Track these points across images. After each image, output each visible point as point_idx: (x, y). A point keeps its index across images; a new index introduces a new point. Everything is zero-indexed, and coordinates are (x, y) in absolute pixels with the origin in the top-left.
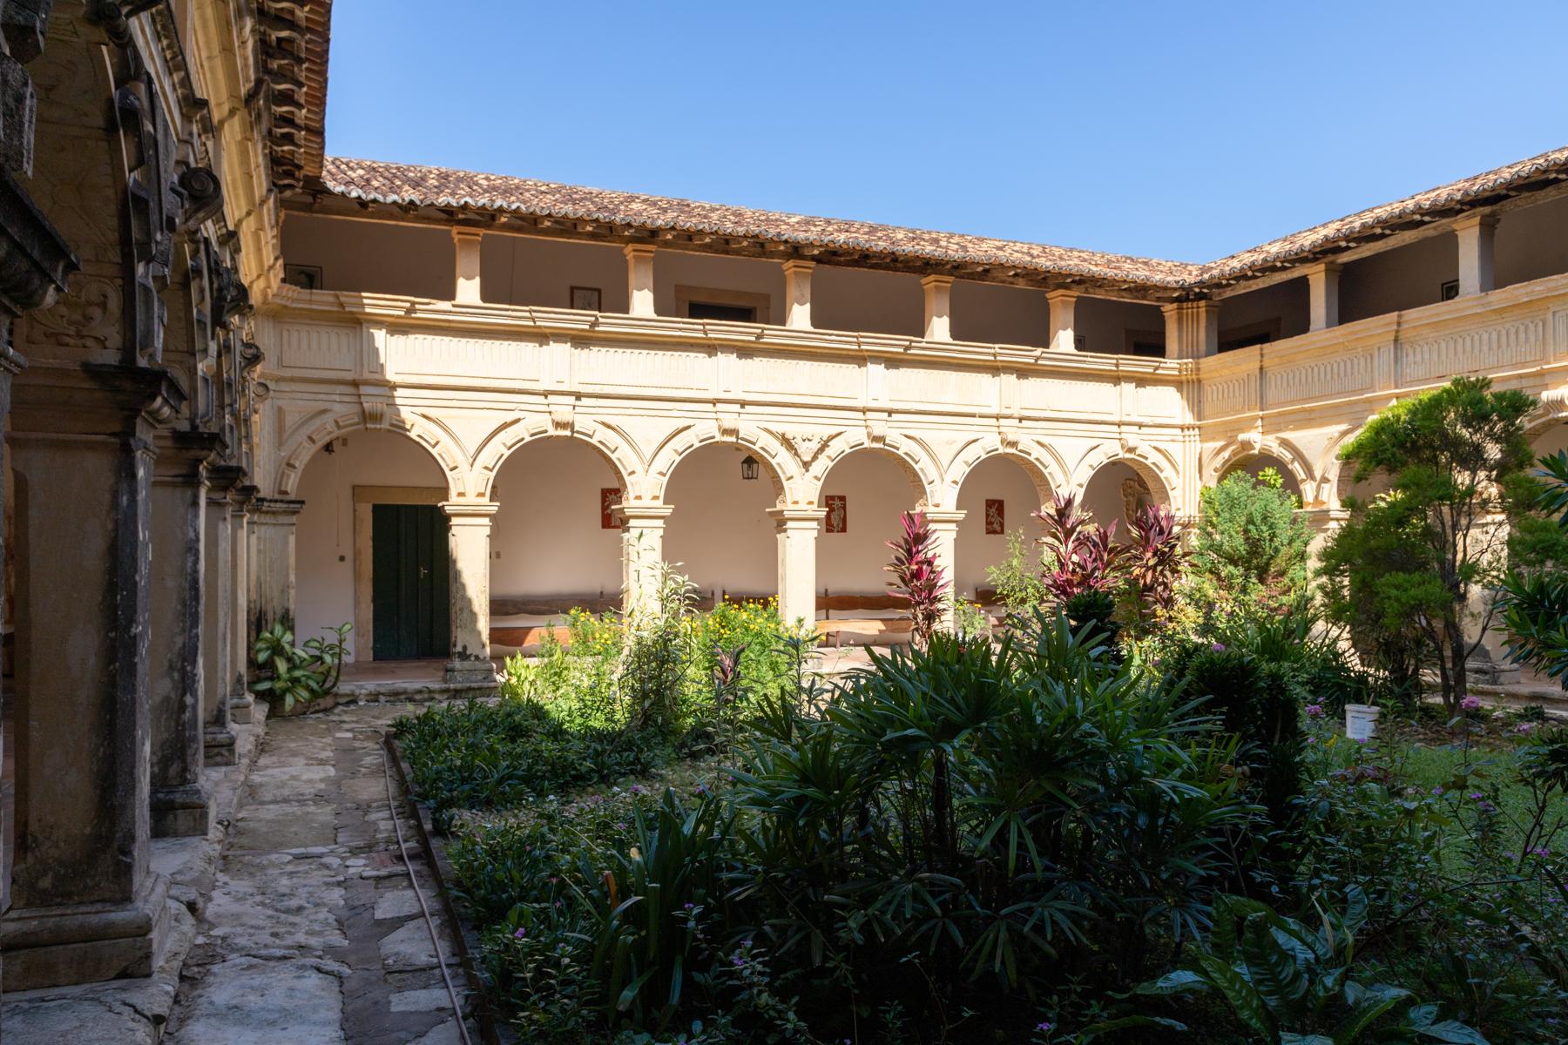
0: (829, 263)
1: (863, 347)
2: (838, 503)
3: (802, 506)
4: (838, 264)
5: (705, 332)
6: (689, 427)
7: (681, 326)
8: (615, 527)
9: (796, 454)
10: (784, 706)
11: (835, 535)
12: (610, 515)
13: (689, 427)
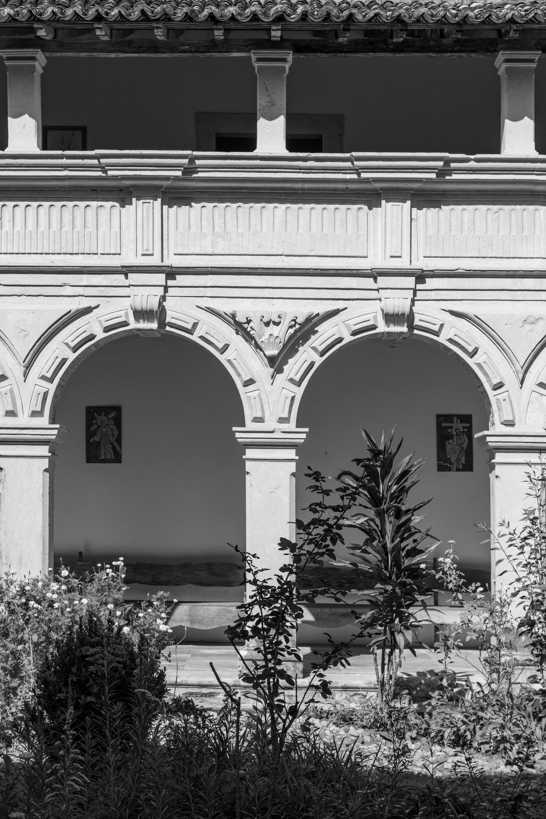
0: (323, 48)
1: (364, 175)
2: (458, 425)
3: (270, 424)
4: (339, 49)
5: (103, 168)
6: (88, 310)
7: (65, 161)
8: (104, 461)
9: (257, 346)
10: (293, 735)
11: (453, 475)
12: (98, 443)
13: (88, 310)
